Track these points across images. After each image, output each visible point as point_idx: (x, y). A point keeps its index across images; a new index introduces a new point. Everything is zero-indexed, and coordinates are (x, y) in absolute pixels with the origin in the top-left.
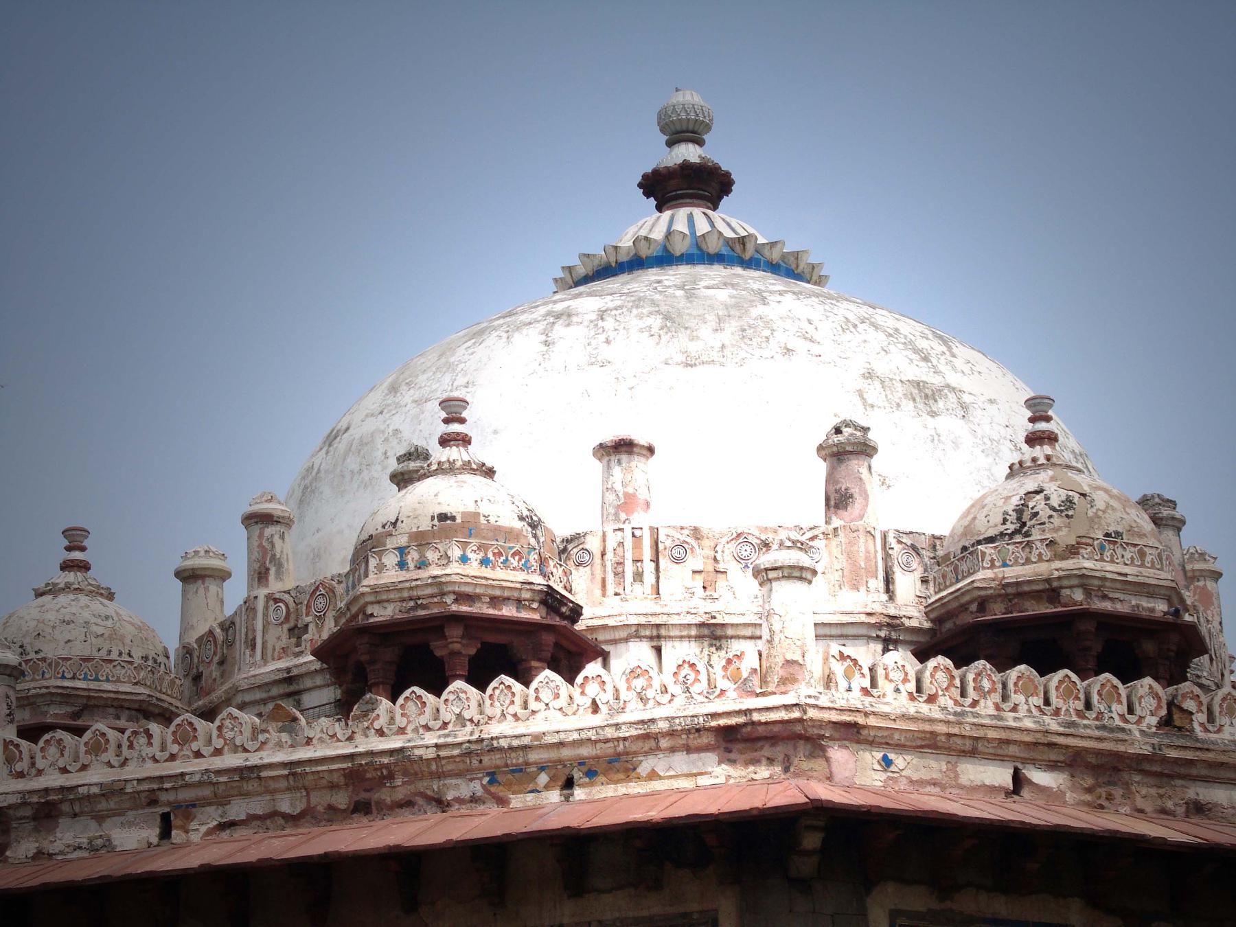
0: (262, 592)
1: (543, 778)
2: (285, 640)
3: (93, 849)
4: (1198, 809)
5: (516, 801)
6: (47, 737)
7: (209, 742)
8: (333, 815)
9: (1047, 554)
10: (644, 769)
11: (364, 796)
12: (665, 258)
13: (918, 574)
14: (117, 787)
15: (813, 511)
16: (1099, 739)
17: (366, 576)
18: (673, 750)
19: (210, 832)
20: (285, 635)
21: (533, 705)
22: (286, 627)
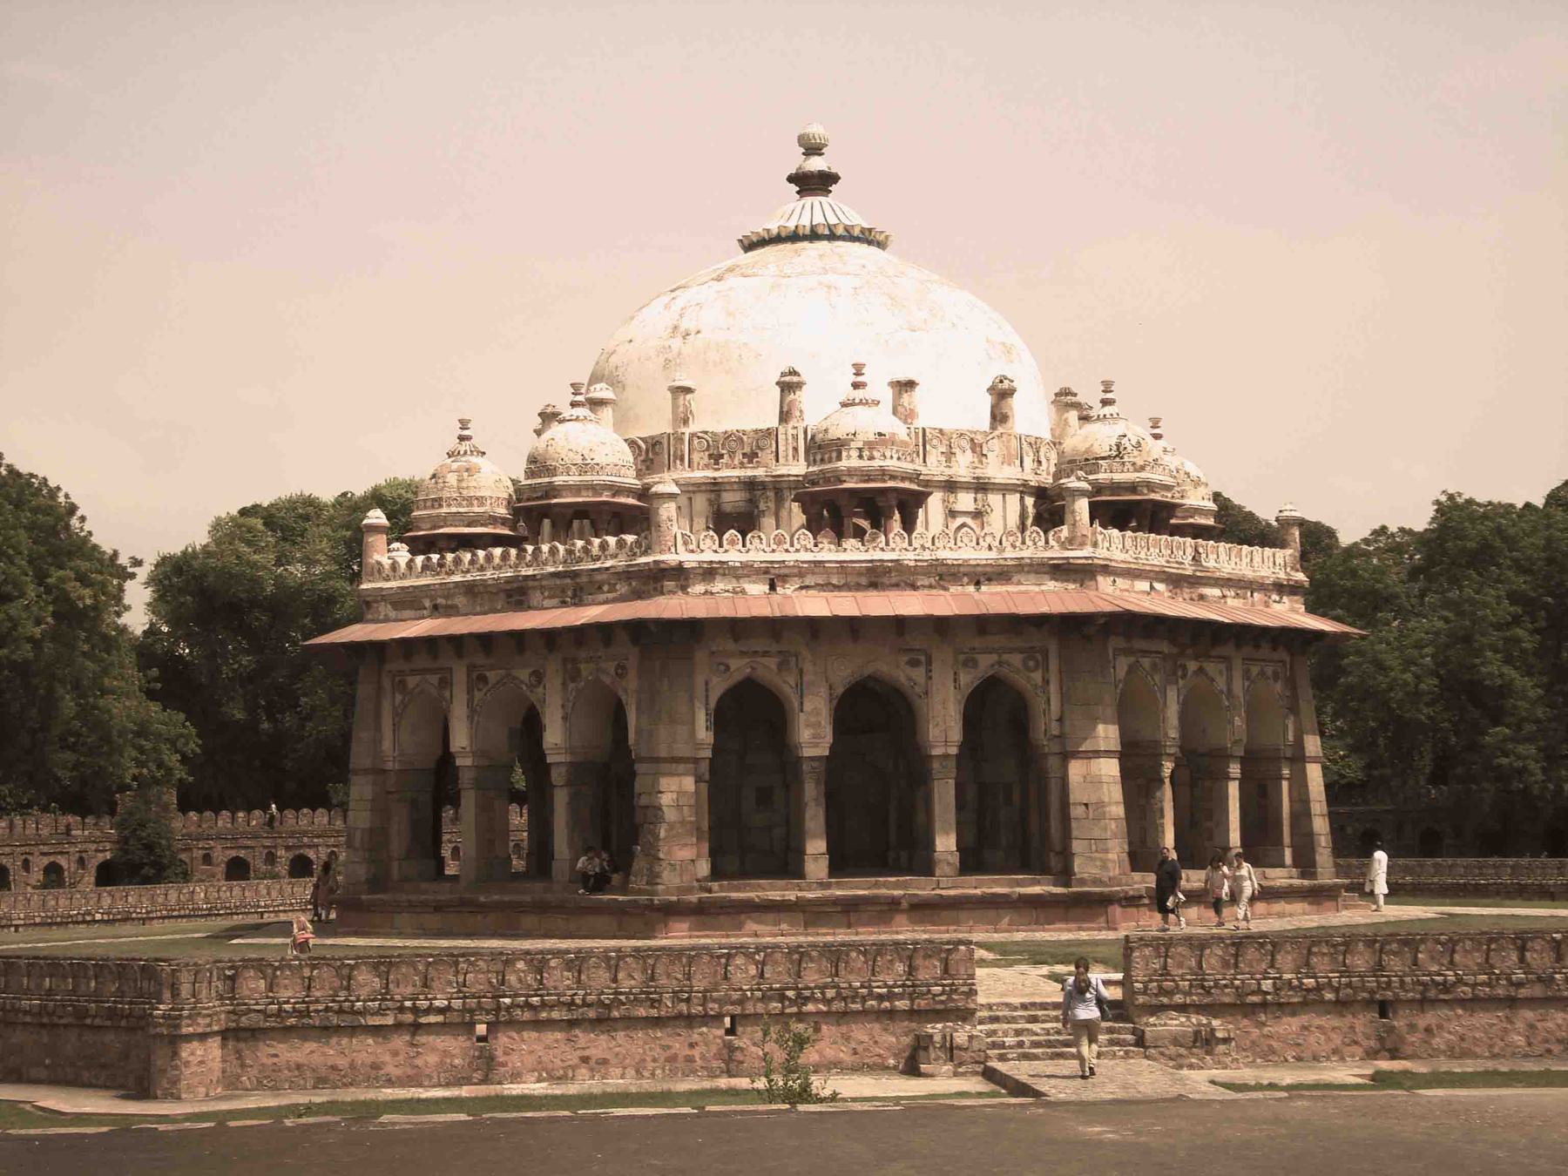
0: (687, 431)
1: (966, 579)
2: (706, 460)
3: (735, 592)
4: (1202, 597)
5: (953, 589)
6: (716, 537)
7: (792, 545)
8: (858, 587)
9: (1131, 469)
10: (1015, 579)
11: (873, 579)
12: (832, 237)
13: (1032, 458)
14: (750, 563)
15: (984, 422)
16: (1178, 568)
17: (839, 458)
18: (1028, 572)
19: (795, 590)
20: (706, 458)
21: (959, 544)
22: (707, 453)
